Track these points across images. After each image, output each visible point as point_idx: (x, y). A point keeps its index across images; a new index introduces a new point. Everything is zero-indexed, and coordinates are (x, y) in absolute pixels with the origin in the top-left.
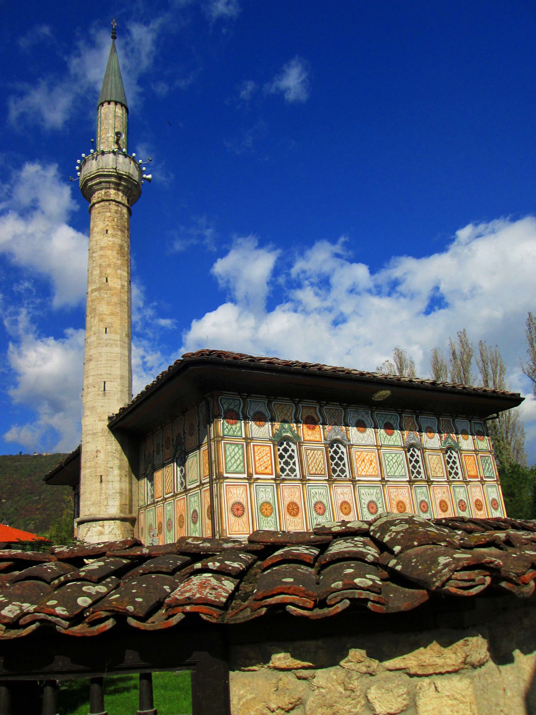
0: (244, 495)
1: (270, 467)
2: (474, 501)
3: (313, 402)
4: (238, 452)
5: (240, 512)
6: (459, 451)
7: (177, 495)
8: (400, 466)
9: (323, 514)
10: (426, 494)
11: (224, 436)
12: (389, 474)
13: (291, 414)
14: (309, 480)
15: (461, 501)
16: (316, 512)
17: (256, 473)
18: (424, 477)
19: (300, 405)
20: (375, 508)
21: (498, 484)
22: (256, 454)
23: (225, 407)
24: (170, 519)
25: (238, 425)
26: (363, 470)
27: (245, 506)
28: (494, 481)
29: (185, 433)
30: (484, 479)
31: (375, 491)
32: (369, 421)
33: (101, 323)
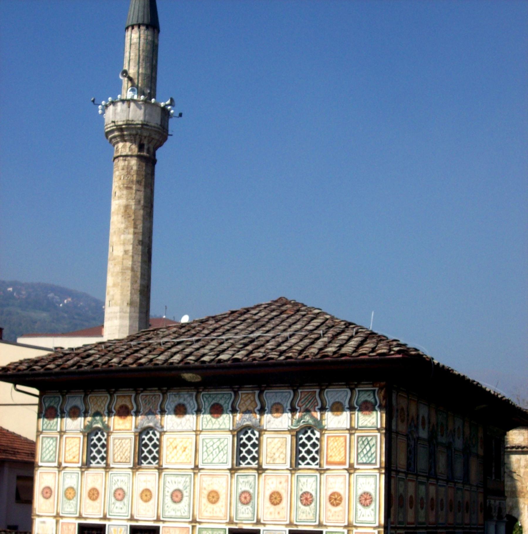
1: (77, 457)
2: (329, 493)
3: (129, 390)
4: (52, 444)
5: (48, 495)
6: (322, 430)
8: (222, 452)
9: (121, 500)
10: (253, 484)
11: (43, 430)
12: (206, 461)
13: (105, 405)
14: (113, 468)
17: (65, 462)
20: (180, 496)
21: (380, 474)
22: (67, 445)
23: (47, 405)
27: (53, 490)
28: (375, 469)
30: (356, 466)
32: (192, 404)
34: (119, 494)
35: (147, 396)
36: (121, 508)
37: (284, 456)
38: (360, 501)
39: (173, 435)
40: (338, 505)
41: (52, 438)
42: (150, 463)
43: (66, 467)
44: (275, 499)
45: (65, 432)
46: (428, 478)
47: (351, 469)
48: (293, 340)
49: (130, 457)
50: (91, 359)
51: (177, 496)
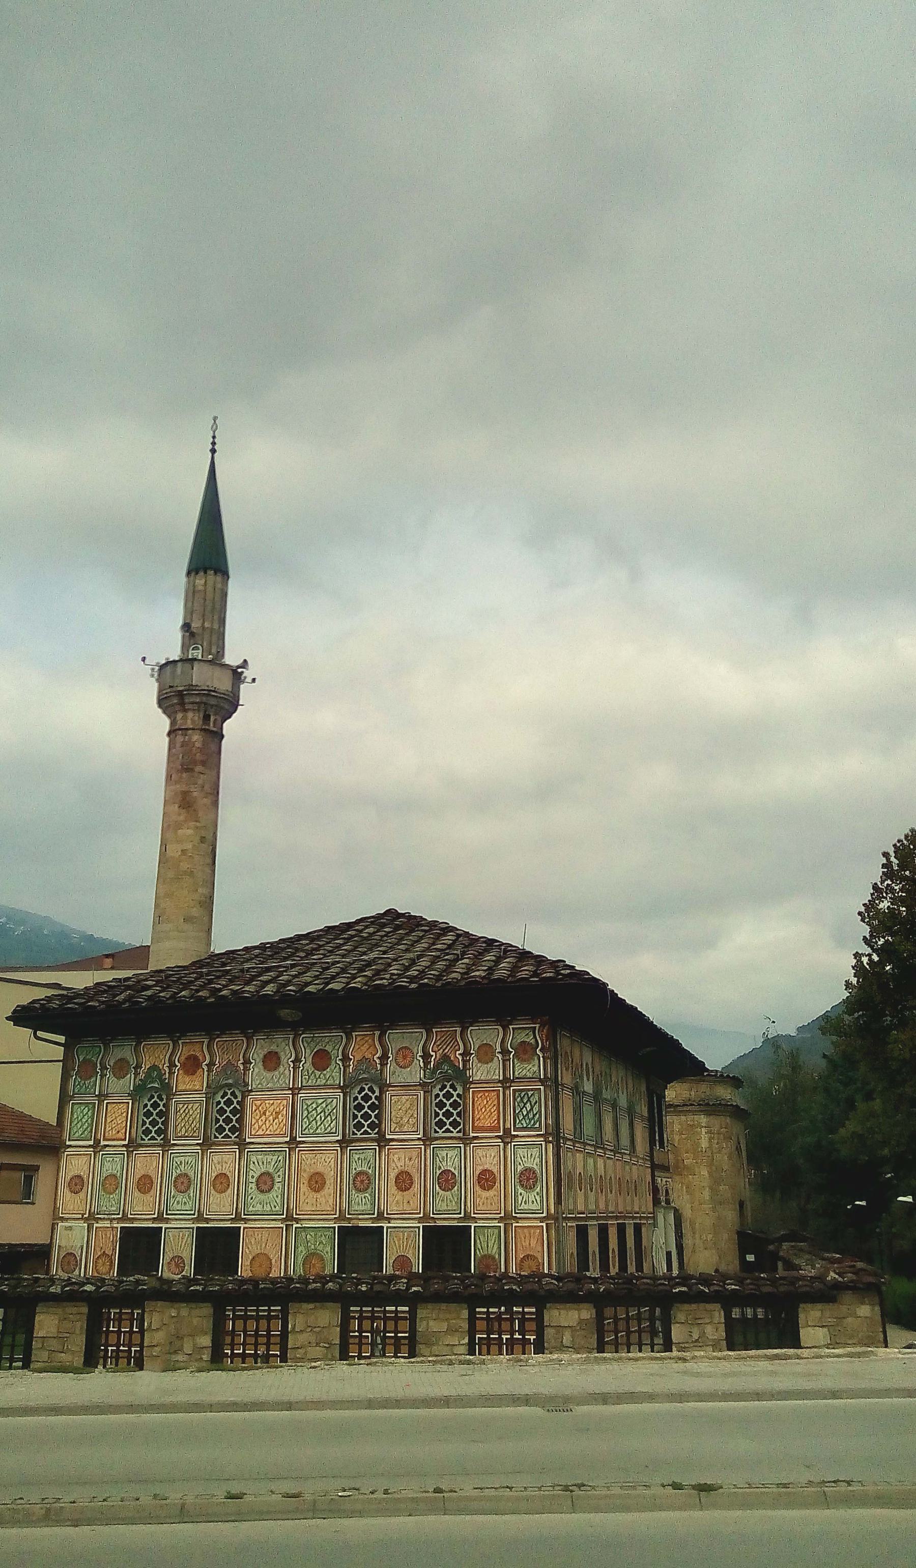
0: (86, 1168)
2: (478, 1172)
6: (466, 1083)
8: (329, 1118)
19: (180, 1042)
21: (547, 1142)
25: (93, 1079)
26: (259, 1128)
28: (538, 1135)
30: (513, 1133)
34: (182, 1183)
36: (185, 1203)
37: (415, 1121)
38: (520, 1181)
40: (490, 1188)
42: (227, 1136)
44: (404, 1181)
45: (107, 1096)
46: (596, 1147)
47: (507, 1137)
48: (424, 962)
49: (198, 1129)
50: (149, 993)
51: (265, 1182)
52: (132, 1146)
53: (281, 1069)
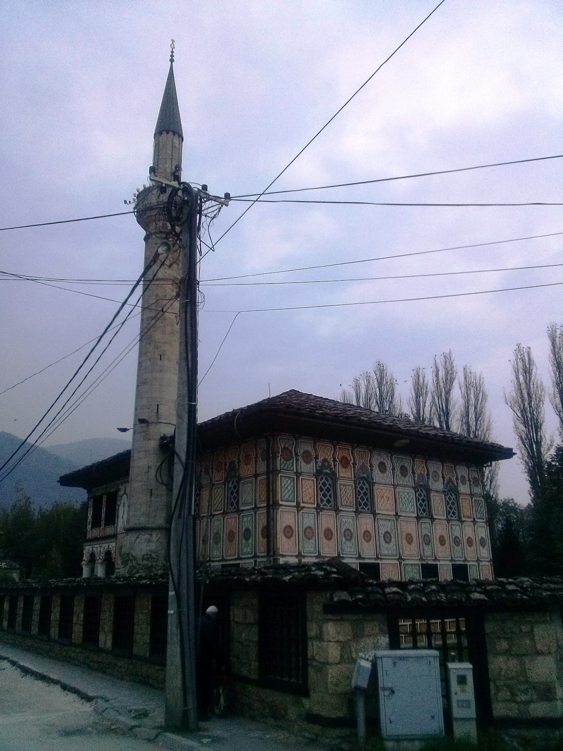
0: (293, 520)
1: (313, 498)
4: (290, 484)
7: (227, 513)
11: (281, 469)
15: (456, 537)
16: (345, 537)
17: (303, 502)
18: (428, 514)
23: (283, 446)
24: (217, 533)
25: (291, 461)
29: (239, 461)
31: (390, 523)
33: (156, 350)
35: (360, 451)
39: (381, 487)
41: (290, 478)
43: (303, 507)
45: (301, 474)
52: (319, 509)
53: (387, 473)
